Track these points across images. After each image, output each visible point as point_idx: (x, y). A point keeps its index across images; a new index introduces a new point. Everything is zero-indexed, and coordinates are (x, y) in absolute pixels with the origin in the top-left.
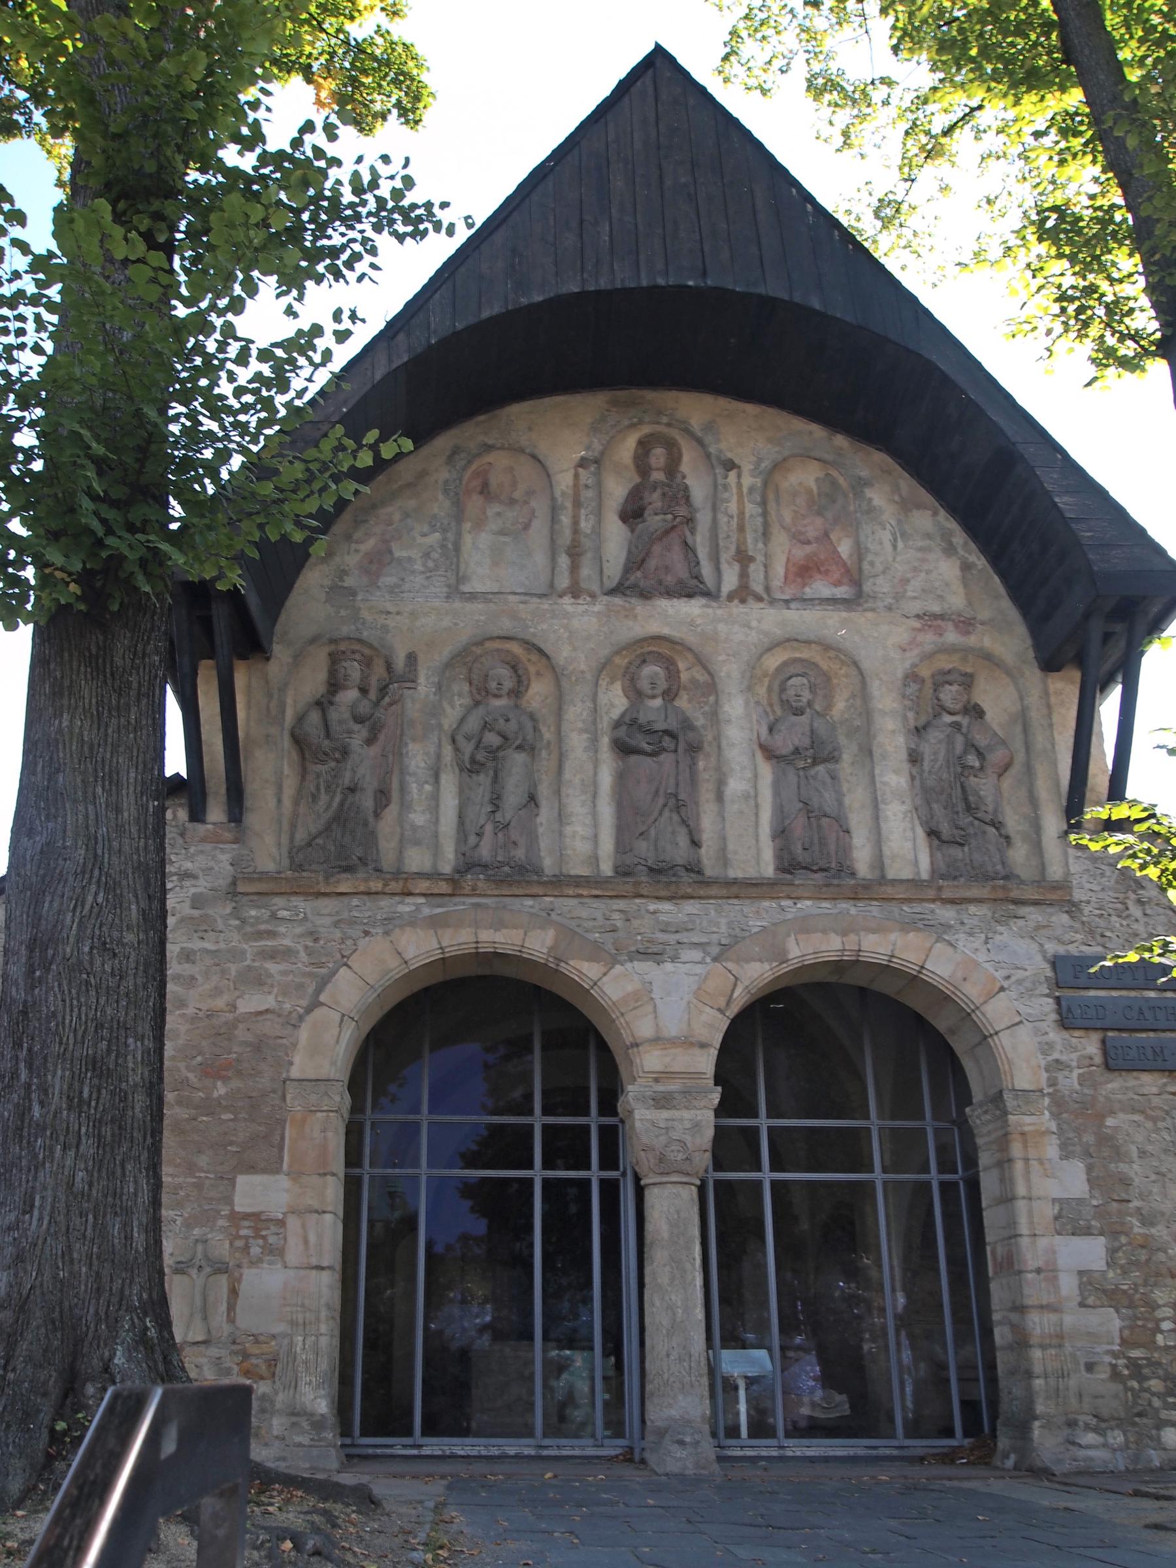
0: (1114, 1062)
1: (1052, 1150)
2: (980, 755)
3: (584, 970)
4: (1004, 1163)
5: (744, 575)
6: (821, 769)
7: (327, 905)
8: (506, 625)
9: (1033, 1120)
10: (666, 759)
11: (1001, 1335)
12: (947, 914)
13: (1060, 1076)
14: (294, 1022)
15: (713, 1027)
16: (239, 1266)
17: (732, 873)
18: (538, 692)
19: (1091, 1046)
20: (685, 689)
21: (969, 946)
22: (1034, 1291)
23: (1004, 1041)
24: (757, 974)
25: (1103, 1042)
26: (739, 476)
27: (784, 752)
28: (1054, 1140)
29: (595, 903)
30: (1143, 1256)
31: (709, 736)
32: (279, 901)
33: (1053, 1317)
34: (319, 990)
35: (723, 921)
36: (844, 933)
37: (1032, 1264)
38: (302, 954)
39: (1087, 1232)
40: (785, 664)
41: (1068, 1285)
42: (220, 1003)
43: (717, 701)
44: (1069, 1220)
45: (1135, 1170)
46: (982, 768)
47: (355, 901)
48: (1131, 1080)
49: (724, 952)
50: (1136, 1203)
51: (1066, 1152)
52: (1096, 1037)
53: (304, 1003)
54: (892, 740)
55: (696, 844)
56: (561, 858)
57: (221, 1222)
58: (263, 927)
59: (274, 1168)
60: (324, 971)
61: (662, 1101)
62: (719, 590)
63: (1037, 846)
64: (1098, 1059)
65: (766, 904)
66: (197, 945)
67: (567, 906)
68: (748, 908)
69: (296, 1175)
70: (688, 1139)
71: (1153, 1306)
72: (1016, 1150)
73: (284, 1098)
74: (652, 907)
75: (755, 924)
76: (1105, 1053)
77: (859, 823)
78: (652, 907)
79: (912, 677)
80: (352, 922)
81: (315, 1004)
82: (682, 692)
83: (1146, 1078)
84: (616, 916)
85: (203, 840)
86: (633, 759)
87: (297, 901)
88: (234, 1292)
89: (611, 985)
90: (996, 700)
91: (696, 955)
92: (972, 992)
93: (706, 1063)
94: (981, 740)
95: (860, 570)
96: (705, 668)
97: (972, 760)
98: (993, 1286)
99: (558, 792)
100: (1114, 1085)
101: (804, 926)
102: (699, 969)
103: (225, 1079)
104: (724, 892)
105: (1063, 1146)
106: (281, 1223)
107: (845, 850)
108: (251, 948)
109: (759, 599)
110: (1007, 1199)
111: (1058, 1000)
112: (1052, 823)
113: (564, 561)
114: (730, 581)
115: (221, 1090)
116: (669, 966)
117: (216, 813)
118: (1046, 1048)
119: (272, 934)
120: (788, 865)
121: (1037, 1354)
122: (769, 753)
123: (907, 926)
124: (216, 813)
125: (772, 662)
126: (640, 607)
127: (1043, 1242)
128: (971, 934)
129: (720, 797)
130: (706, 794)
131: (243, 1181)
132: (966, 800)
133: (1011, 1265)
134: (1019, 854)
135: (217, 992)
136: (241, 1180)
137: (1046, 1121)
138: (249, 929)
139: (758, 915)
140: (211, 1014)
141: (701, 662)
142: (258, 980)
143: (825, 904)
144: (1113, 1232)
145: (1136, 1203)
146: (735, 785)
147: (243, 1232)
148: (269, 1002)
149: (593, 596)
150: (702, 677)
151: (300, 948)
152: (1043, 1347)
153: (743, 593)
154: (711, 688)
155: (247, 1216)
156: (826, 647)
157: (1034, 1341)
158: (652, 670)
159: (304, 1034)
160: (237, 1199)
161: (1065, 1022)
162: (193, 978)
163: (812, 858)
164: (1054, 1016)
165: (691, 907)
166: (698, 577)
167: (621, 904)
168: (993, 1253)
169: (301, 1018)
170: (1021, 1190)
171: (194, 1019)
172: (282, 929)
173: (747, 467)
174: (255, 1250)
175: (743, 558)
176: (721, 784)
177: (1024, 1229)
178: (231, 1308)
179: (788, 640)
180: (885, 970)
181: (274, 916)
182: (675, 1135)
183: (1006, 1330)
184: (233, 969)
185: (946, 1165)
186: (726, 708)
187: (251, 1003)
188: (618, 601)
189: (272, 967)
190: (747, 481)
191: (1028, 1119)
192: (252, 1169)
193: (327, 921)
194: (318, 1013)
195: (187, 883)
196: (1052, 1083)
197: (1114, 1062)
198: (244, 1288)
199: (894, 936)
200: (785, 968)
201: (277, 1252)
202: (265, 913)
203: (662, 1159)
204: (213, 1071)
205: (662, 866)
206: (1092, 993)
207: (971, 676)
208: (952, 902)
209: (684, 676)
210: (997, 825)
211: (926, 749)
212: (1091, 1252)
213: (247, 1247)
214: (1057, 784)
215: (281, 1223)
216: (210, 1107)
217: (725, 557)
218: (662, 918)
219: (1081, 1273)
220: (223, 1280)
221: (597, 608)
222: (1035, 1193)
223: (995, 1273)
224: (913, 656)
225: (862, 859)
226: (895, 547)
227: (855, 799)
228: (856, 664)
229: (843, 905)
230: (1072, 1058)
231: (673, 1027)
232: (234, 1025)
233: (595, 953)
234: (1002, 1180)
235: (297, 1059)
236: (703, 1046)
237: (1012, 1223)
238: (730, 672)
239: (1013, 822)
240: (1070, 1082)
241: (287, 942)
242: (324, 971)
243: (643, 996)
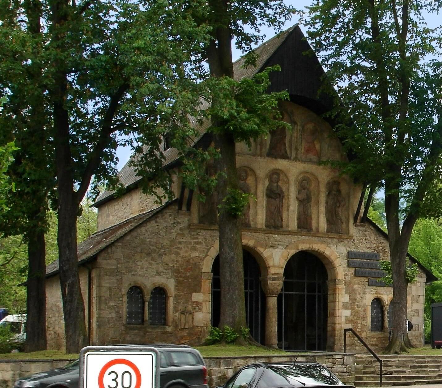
0: (356, 275)
1: (344, 293)
2: (339, 203)
3: (260, 250)
4: (334, 294)
5: (296, 154)
6: (308, 204)
7: (209, 232)
8: (246, 163)
9: (341, 287)
10: (278, 200)
11: (329, 329)
12: (329, 240)
13: (346, 277)
14: (203, 259)
15: (284, 263)
16: (193, 312)
17: (290, 229)
18: (250, 180)
19: (352, 271)
20: (281, 180)
21: (333, 248)
22: (338, 320)
23: (338, 269)
24: (293, 252)
25: (355, 270)
26: (297, 127)
27: (301, 199)
28: (344, 290)
29: (262, 234)
30: (357, 314)
31: (286, 194)
32: (198, 231)
33: (340, 325)
34: (207, 252)
35: (287, 240)
36: (310, 244)
37: (337, 315)
38: (204, 243)
39: (347, 308)
40: (302, 178)
41: (343, 319)
42: (187, 254)
43: (289, 187)
44: (345, 307)
45: (358, 297)
46: (339, 206)
47: (214, 231)
48: (359, 279)
49: (286, 247)
50: (357, 303)
51: (346, 294)
52: (354, 269)
53: (204, 255)
54: (323, 199)
55: (282, 220)
56: (256, 223)
57: (190, 303)
58: (195, 236)
59: (199, 291)
60: (208, 247)
61: (274, 279)
62: (291, 157)
63: (348, 226)
64: (354, 274)
65: (296, 236)
66: (182, 240)
67: (257, 234)
68: (292, 237)
69: (204, 293)
70: (278, 287)
71: (357, 323)
72: (337, 292)
73: (201, 276)
74: (273, 236)
75: (293, 241)
76: (355, 272)
77: (314, 217)
78: (273, 236)
79: (328, 183)
80: (213, 236)
81: (207, 255)
82: (280, 181)
83: (362, 278)
84: (266, 237)
85: (182, 214)
86: (270, 199)
87: (203, 231)
88: (193, 318)
89: (266, 253)
90: (344, 188)
91: (281, 247)
92: (333, 258)
93: (282, 271)
94: (340, 199)
95: (320, 155)
96: (287, 178)
97: (338, 205)
98: (329, 319)
99: (256, 208)
100: (356, 280)
101: (303, 242)
102: (282, 251)
103: (189, 272)
104: (288, 233)
105: (346, 291)
106: (201, 303)
107: (311, 224)
108: (192, 241)
109: (299, 161)
110: (334, 301)
111: (348, 261)
112: (351, 221)
113: (259, 147)
114: (293, 156)
115: (188, 274)
116: (276, 250)
117: (184, 208)
118: (345, 271)
119: (197, 238)
120: (299, 226)
121: (337, 332)
122: (298, 199)
123: (322, 242)
124: (184, 208)
125: (301, 176)
126: (274, 161)
127: (340, 311)
128: (333, 245)
129: (288, 211)
130: (285, 208)
131: (194, 294)
132: (335, 214)
133: (333, 315)
134: (344, 226)
135: (186, 252)
136: (194, 294)
137: (343, 286)
138: (193, 237)
139: (294, 239)
140: (186, 257)
141: (286, 175)
142: (195, 249)
143: (307, 237)
144: (352, 309)
145: (357, 303)
146: (291, 208)
147: (194, 305)
148: (197, 254)
149: (265, 157)
150: (285, 180)
151: (203, 242)
152: (338, 331)
153: (296, 159)
154: (288, 182)
155: (194, 302)
156: (312, 174)
157: (337, 330)
158: (275, 176)
159: (205, 262)
160: (193, 298)
161: (349, 265)
162: (181, 248)
163: (305, 225)
164: (347, 264)
165: (281, 236)
166: (286, 152)
167: (268, 235)
168: (329, 313)
169: (204, 258)
170: (337, 300)
171: (182, 258)
172: (199, 237)
173: (299, 124)
174: (197, 309)
175: (297, 149)
176: (288, 207)
177: (337, 308)
178: (193, 321)
179: (305, 172)
180: (317, 252)
181: (197, 234)
182: (275, 287)
183: (331, 328)
184: (190, 246)
185: (319, 292)
186: (291, 189)
187: (195, 254)
188: (269, 159)
189: (198, 246)
190: (299, 128)
191: (340, 286)
192: (195, 292)
193: (209, 236)
194: (207, 257)
195: (179, 225)
196: (345, 278)
197: (356, 275)
198: (194, 317)
199: (319, 245)
200: (298, 251)
201: (200, 310)
202: (195, 233)
203: (273, 291)
204: (186, 270)
205: (275, 225)
206: (354, 260)
207: (339, 183)
208: (331, 238)
209: (281, 178)
210: (341, 220)
211: (329, 201)
212: (347, 313)
213: (195, 308)
214: (354, 211)
215: (201, 303)
216: (187, 278)
217: (293, 149)
218: (275, 238)
219: (346, 317)
220: (191, 316)
221: (266, 160)
222: (340, 301)
223: (329, 316)
224: (329, 178)
225: (314, 225)
226: (328, 149)
227: (314, 211)
228: (317, 179)
229: (310, 237)
230: (349, 273)
231: (276, 263)
232: (189, 259)
233: (262, 246)
234: (333, 298)
235: (204, 268)
236: (282, 268)
237: (335, 306)
238: (292, 178)
239: (343, 219)
240: (348, 278)
241: (200, 240)
242: (208, 247)
243: (271, 256)
